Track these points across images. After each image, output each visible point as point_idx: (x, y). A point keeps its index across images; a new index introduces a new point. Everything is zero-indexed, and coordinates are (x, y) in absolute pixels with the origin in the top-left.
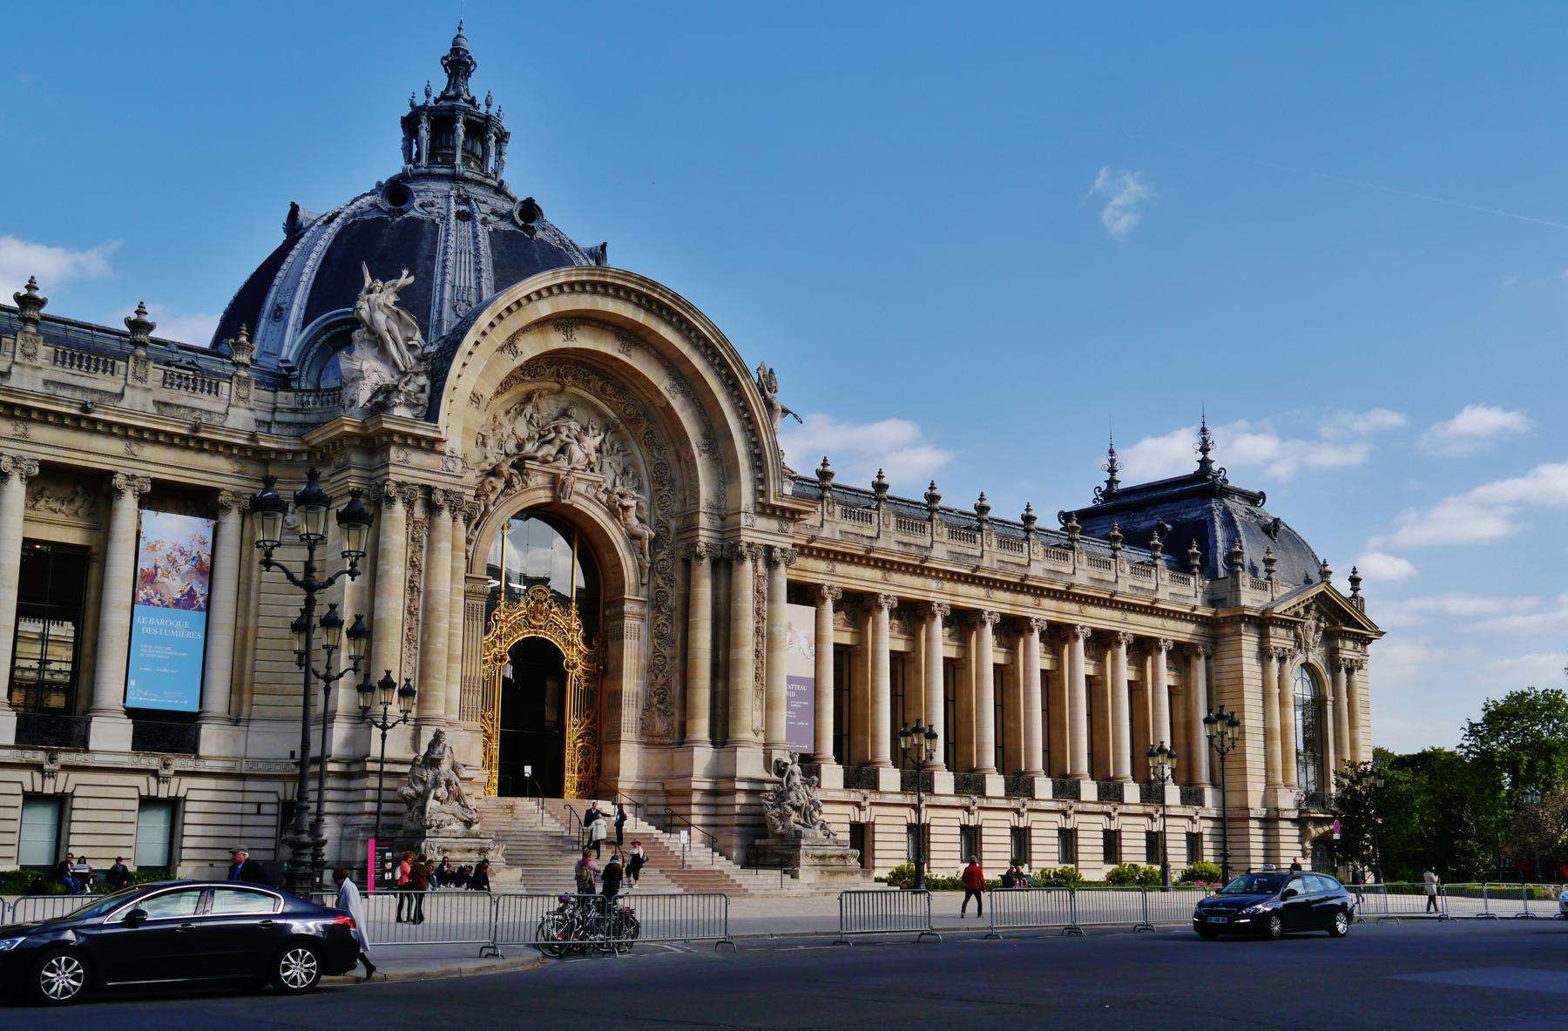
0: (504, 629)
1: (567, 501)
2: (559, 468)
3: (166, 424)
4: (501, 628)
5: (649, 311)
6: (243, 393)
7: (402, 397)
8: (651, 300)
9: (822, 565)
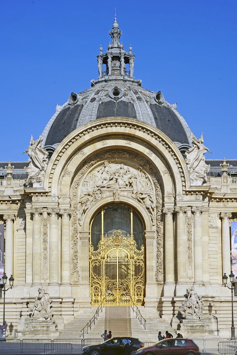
0: (104, 246)
2: (114, 189)
4: (103, 247)
6: (9, 183)
7: (35, 180)
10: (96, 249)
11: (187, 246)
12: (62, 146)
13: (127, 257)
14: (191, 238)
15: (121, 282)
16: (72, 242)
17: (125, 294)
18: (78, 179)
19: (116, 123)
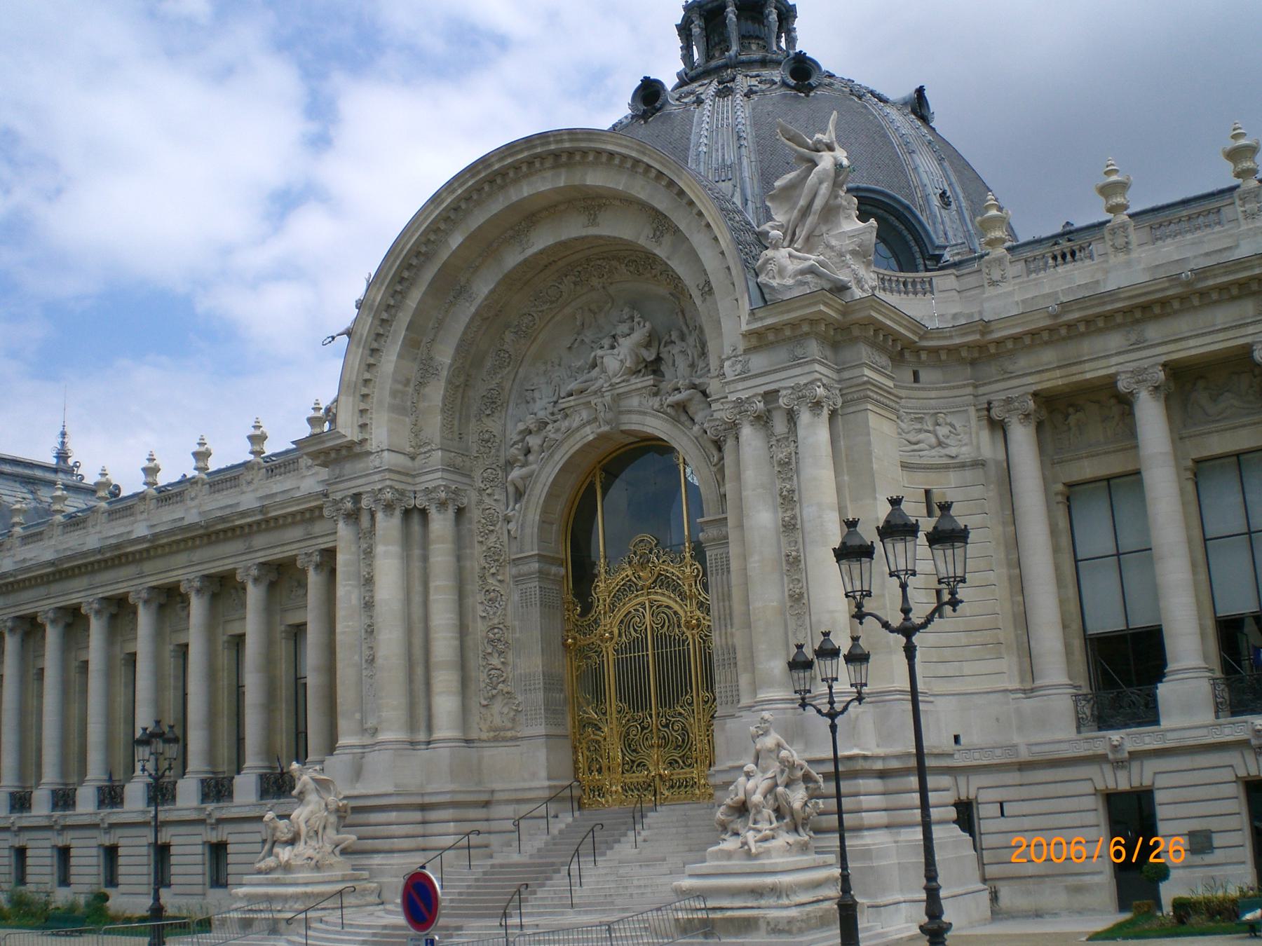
0: (608, 601)
1: (605, 428)
2: (595, 393)
3: (310, 501)
4: (605, 601)
5: (569, 165)
8: (556, 155)
9: (1115, 341)
10: (587, 608)
11: (783, 554)
12: (382, 284)
13: (679, 626)
14: (794, 517)
15: (666, 719)
16: (480, 597)
17: (679, 760)
18: (492, 386)
19: (522, 161)
